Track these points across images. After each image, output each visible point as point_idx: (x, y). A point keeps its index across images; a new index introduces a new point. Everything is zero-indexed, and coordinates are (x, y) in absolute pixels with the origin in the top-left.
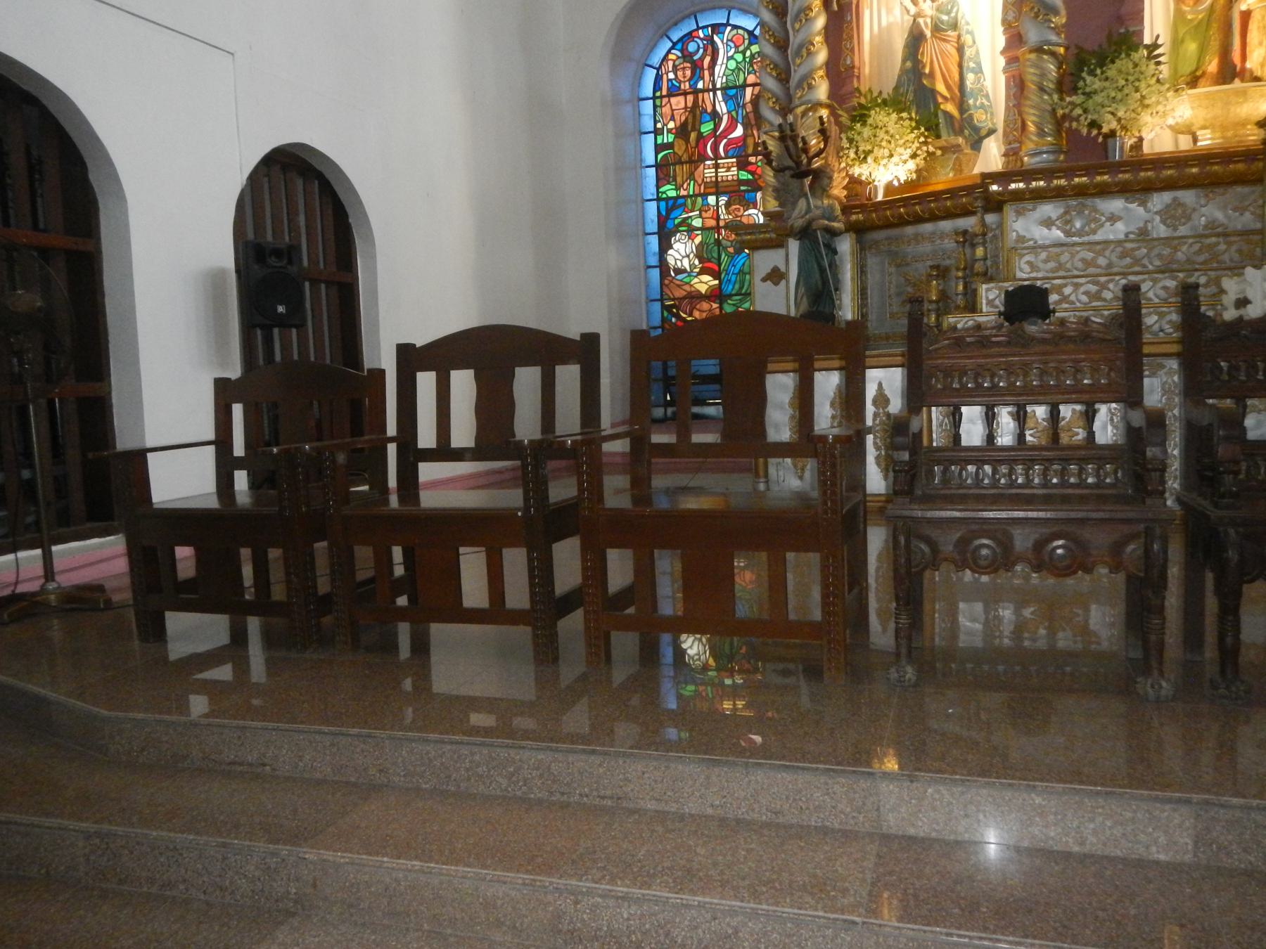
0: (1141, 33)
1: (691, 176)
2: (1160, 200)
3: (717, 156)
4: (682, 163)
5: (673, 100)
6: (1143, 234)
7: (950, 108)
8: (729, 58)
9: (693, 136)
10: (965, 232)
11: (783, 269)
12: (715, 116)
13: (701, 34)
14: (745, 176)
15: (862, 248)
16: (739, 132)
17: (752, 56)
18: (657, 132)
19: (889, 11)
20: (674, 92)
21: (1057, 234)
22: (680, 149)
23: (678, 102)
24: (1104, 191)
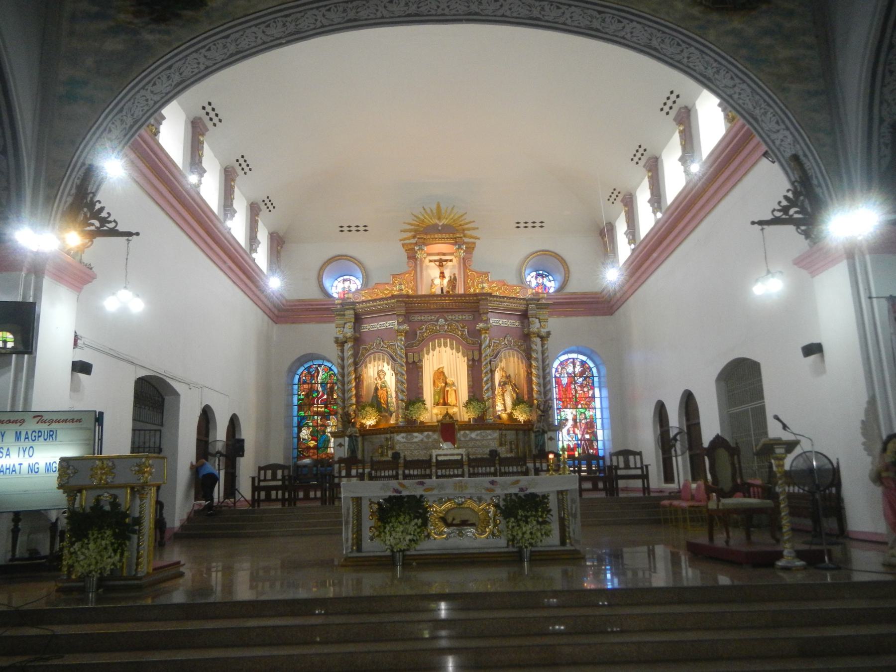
1: (309, 410)
2: (426, 433)
3: (318, 404)
4: (305, 405)
6: (422, 440)
7: (385, 406)
8: (323, 375)
11: (343, 443)
12: (318, 392)
13: (314, 366)
14: (327, 410)
15: (363, 440)
16: (325, 397)
17: (330, 375)
18: (299, 395)
20: (304, 383)
22: (306, 401)
23: (306, 386)
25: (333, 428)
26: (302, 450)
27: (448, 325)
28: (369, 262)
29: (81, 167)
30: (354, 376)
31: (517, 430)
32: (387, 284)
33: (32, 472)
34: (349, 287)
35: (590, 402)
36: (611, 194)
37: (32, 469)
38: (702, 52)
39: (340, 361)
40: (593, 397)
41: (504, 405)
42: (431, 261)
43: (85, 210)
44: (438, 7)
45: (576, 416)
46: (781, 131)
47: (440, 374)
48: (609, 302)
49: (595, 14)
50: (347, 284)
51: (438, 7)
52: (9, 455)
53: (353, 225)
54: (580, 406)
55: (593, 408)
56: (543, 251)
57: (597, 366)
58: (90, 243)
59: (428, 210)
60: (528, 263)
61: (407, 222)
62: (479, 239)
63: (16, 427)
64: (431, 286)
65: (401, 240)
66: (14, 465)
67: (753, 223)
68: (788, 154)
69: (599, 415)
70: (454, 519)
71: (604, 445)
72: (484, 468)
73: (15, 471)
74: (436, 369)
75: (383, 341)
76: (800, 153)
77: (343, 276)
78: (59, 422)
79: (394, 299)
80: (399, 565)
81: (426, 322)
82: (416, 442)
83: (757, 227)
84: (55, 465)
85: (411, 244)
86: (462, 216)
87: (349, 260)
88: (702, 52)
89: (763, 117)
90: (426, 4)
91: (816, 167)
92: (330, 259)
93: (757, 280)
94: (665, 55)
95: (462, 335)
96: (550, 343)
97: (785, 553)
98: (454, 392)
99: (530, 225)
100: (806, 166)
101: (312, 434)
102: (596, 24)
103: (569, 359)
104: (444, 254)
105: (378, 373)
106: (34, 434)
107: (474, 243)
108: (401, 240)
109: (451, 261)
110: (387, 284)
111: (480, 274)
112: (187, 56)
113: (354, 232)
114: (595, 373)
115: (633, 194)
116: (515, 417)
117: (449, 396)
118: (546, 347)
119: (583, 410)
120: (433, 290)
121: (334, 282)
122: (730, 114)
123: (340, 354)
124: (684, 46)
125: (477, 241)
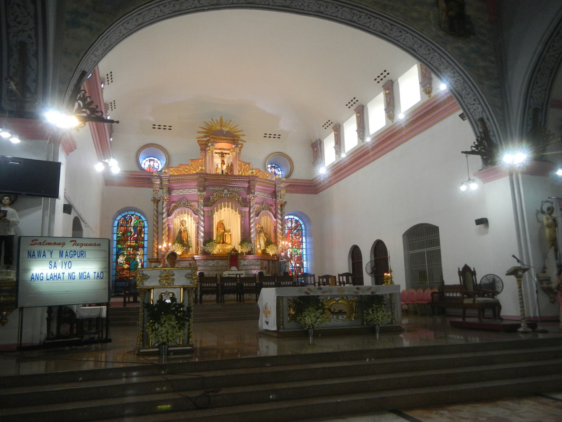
0: (213, 238)
1: (125, 244)
2: (216, 261)
3: (131, 240)
5: (122, 228)
6: (213, 265)
7: (186, 243)
9: (126, 235)
10: (190, 263)
12: (131, 232)
13: (129, 215)
14: (137, 245)
16: (136, 236)
17: (140, 221)
18: (117, 234)
19: (175, 226)
20: (121, 226)
21: (203, 264)
23: (122, 228)
24: (209, 260)
25: (141, 256)
26: (119, 269)
27: (230, 194)
28: (171, 150)
29: (80, 72)
30: (167, 223)
31: (269, 261)
32: (187, 165)
33: (71, 279)
34: (153, 165)
35: (300, 245)
36: (326, 123)
37: (71, 277)
38: (441, 56)
39: (155, 213)
40: (302, 242)
41: (260, 244)
42: (216, 153)
43: (80, 101)
44: (303, 5)
45: (292, 253)
46: (476, 105)
47: (221, 224)
48: (315, 186)
49: (388, 25)
50: (152, 163)
51: (303, 5)
52: (56, 267)
53: (162, 124)
54: (294, 247)
55: (301, 248)
56: (279, 152)
57: (304, 224)
58: (83, 125)
59: (215, 122)
60: (269, 159)
61: (201, 126)
62: (245, 142)
63: (59, 248)
64: (217, 169)
65: (197, 138)
66: (59, 274)
67: (463, 152)
68: (477, 117)
69: (304, 253)
70: (335, 310)
71: (307, 270)
72: (266, 283)
73: (60, 278)
74: (219, 221)
75: (187, 202)
76: (485, 118)
77: (149, 157)
78: (86, 245)
79: (197, 175)
80: (311, 336)
81: (216, 191)
82: (211, 266)
83: (464, 155)
84: (85, 274)
85: (203, 141)
86: (235, 126)
87: (157, 147)
88: (441, 56)
89: (466, 96)
90: (296, 1)
91: (493, 125)
92: (145, 145)
93: (462, 183)
94: (418, 54)
95: (238, 200)
96: (286, 209)
97: (522, 324)
98: (229, 236)
99: (272, 136)
100: (487, 125)
101: (126, 260)
102: (386, 31)
103: (289, 218)
104: (224, 149)
105: (181, 222)
106: (71, 253)
107: (242, 144)
108: (197, 138)
109: (229, 154)
110: (187, 165)
111: (246, 164)
112: (151, 8)
113: (162, 130)
114: (303, 229)
115: (341, 124)
116: (268, 252)
117: (227, 238)
118: (283, 211)
119: (296, 250)
120: (218, 172)
121: (143, 160)
122: (427, 89)
123: (155, 208)
124: (432, 51)
125: (244, 143)
